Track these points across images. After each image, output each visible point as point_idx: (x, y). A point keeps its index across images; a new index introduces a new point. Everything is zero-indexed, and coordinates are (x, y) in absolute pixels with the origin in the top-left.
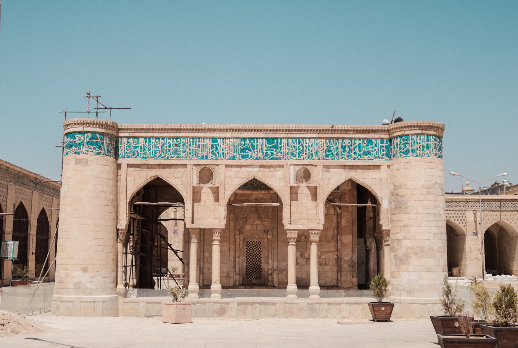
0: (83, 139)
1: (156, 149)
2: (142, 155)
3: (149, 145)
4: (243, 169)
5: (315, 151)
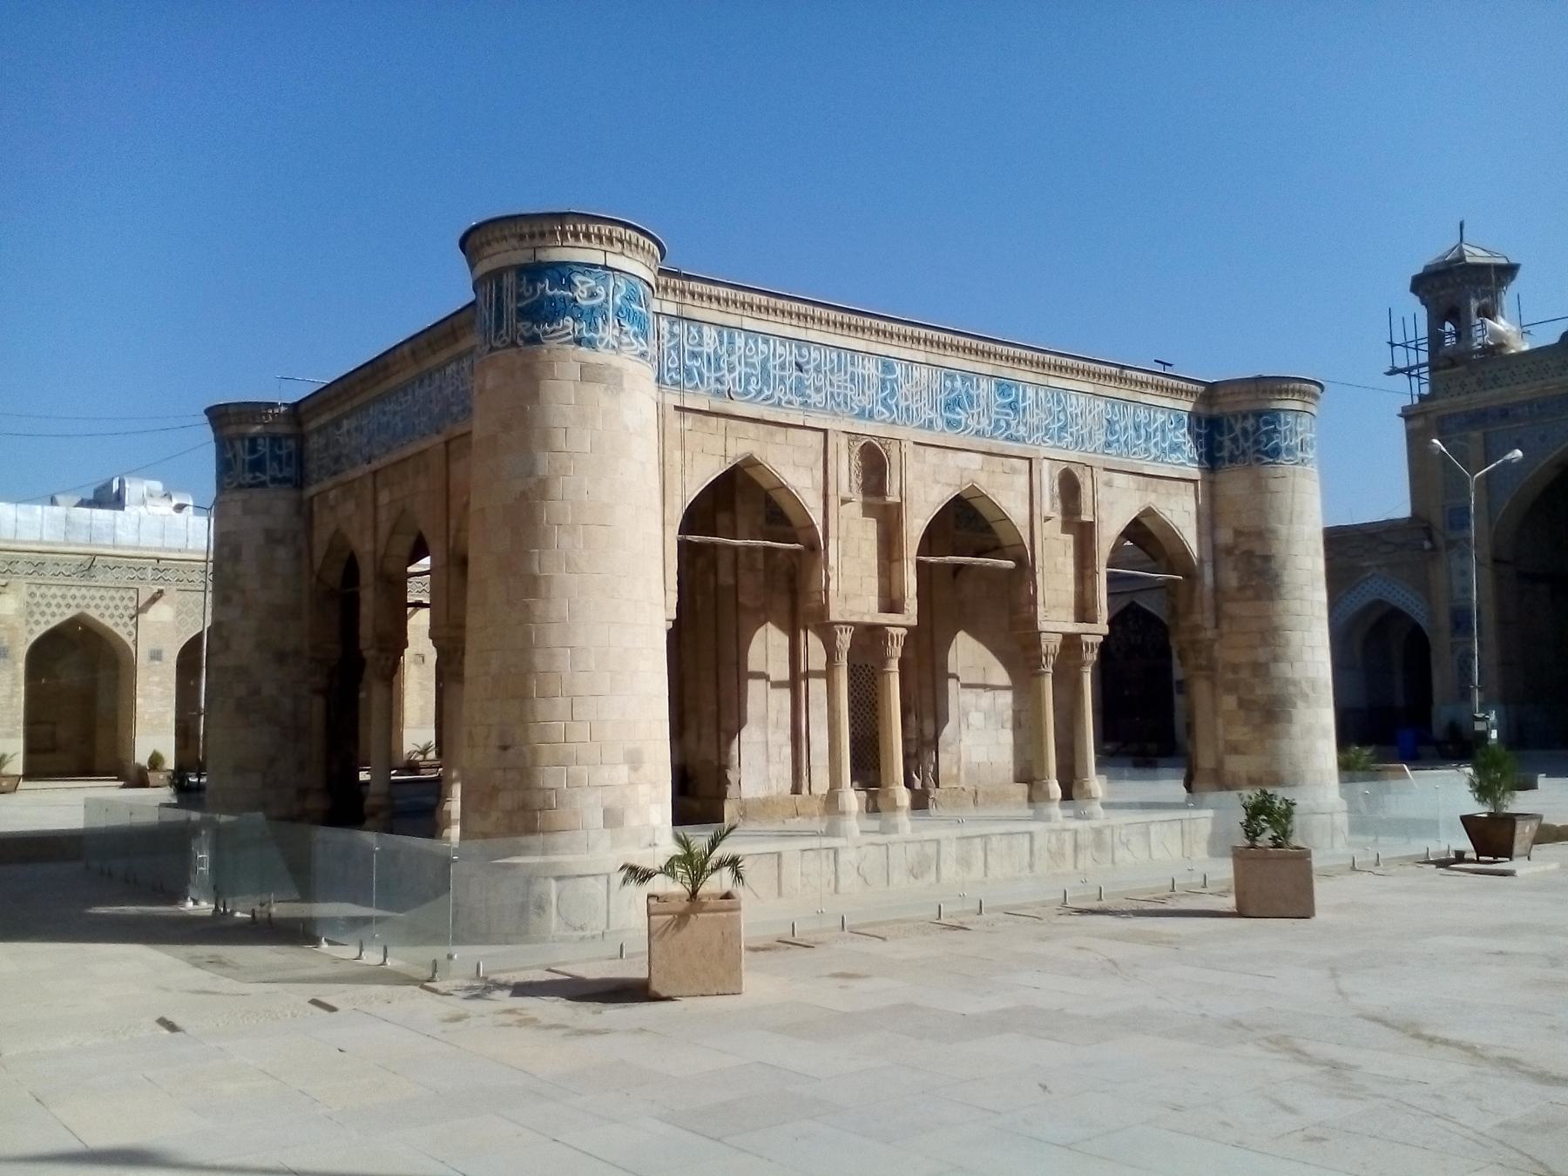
0: (603, 294)
1: (748, 370)
2: (714, 386)
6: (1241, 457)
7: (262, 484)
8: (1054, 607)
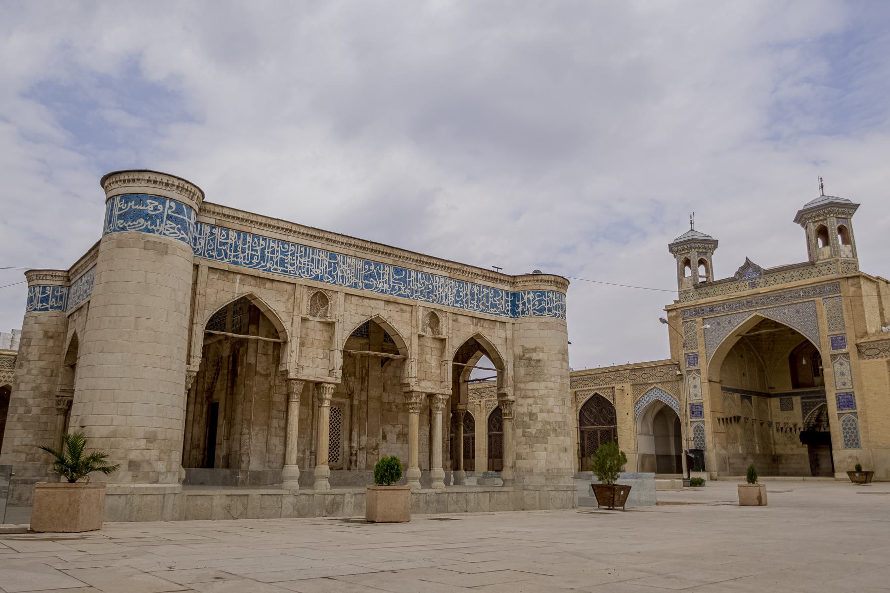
1: (253, 253)
3: (244, 244)
4: (366, 301)
5: (445, 294)
6: (527, 312)
7: (46, 309)
8: (424, 380)
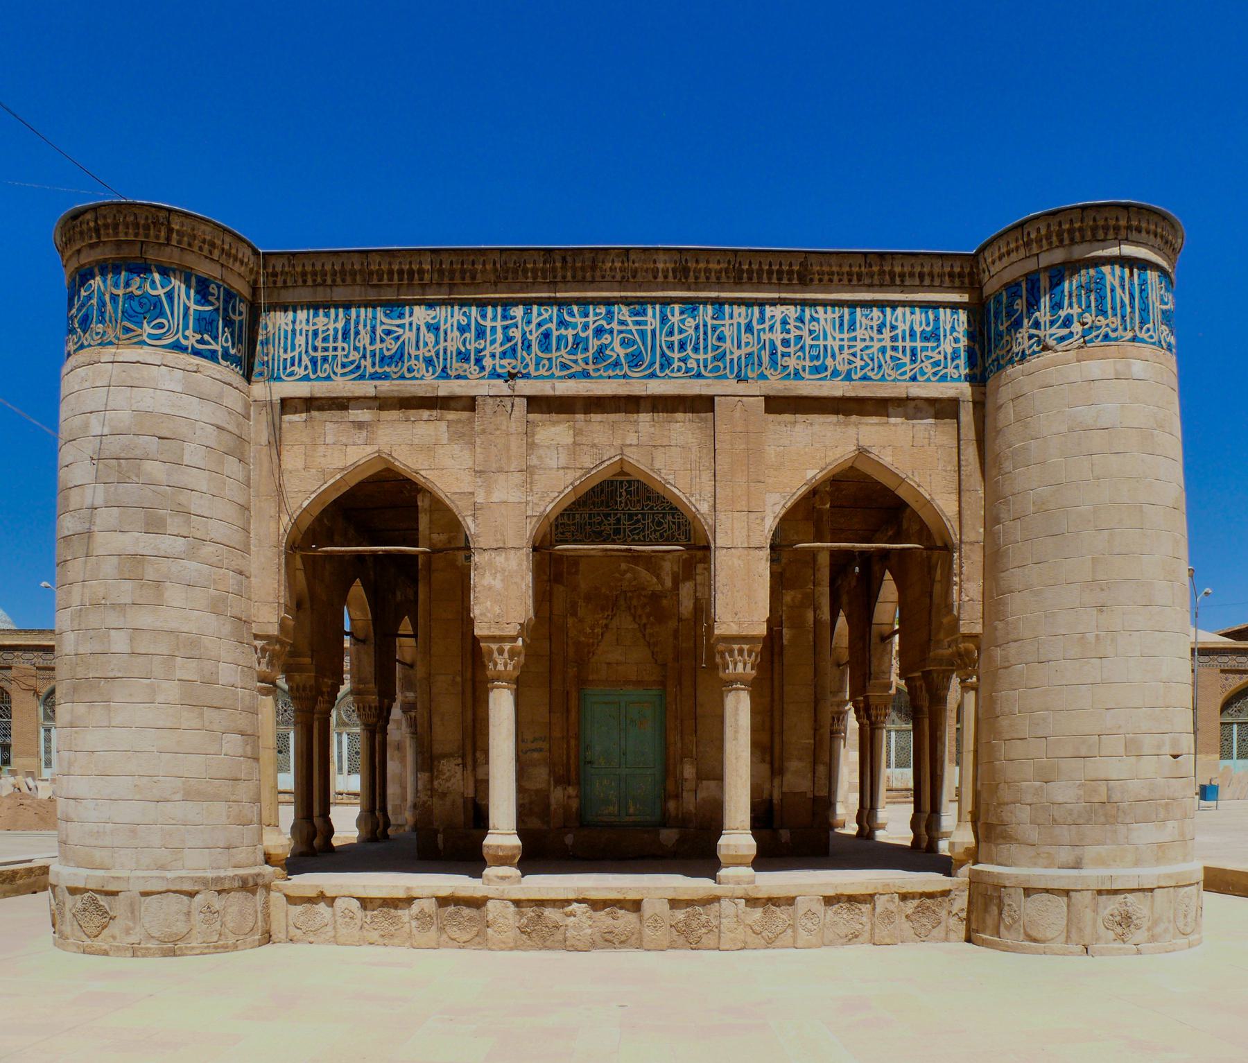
7: (212, 356)
